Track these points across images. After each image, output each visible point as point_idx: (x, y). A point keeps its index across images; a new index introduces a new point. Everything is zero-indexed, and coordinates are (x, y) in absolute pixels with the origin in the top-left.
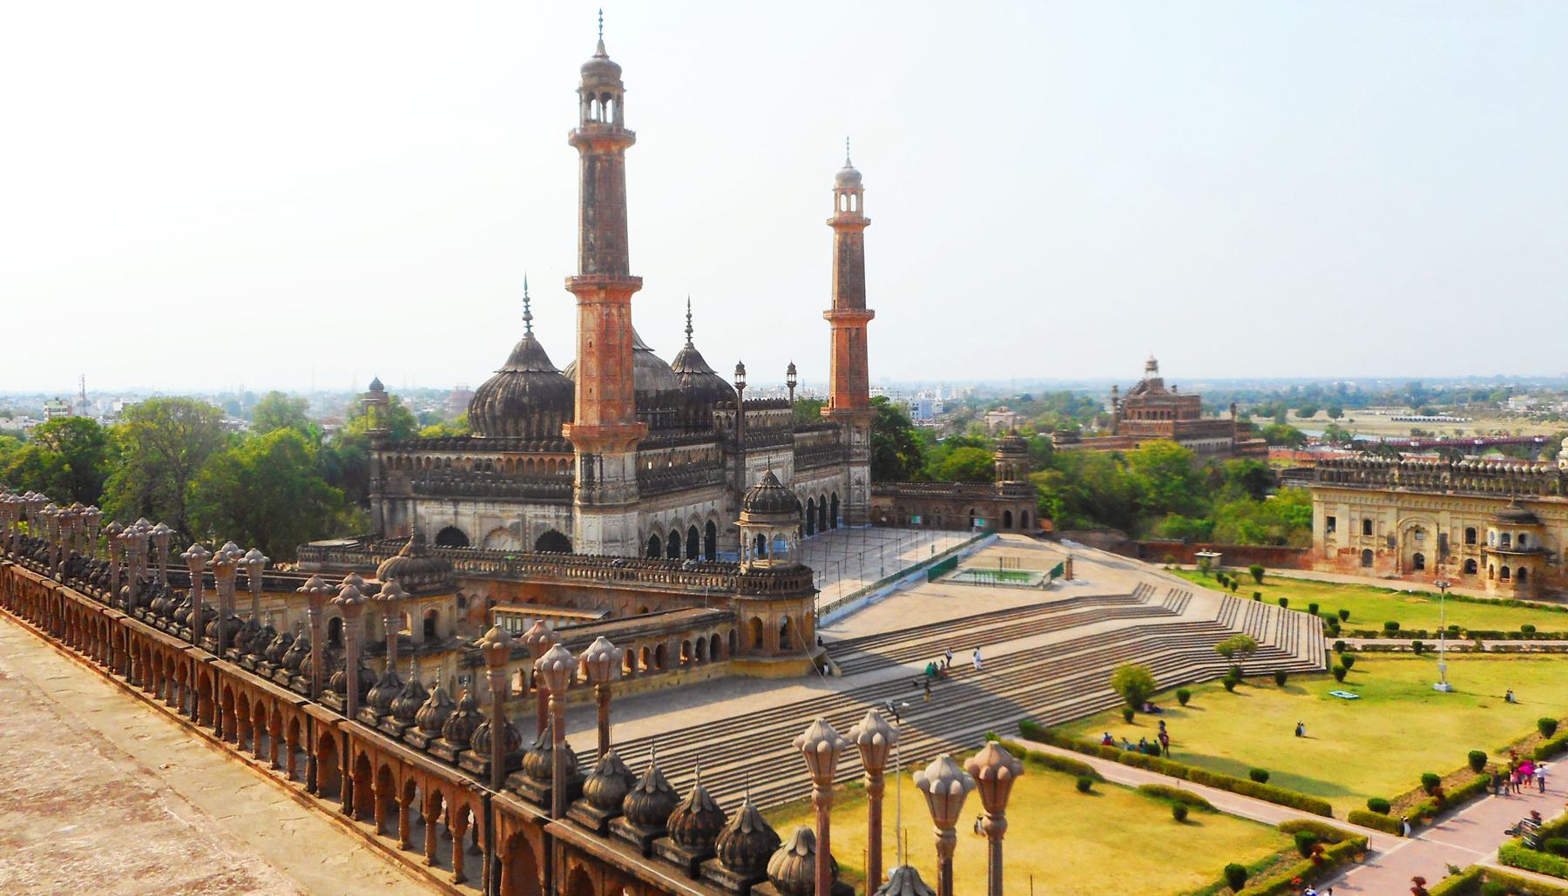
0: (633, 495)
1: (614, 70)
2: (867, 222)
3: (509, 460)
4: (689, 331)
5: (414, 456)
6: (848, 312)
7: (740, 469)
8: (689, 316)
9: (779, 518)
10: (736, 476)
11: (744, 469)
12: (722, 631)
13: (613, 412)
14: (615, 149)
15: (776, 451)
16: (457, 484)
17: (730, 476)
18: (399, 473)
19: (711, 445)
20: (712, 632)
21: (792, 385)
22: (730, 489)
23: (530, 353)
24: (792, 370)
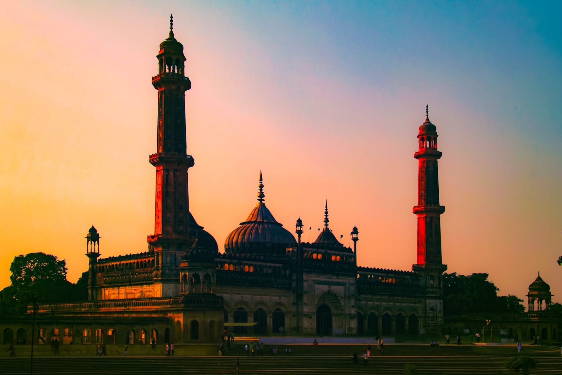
4: (327, 221)
7: (300, 280)
8: (326, 213)
11: (302, 280)
17: (294, 284)
19: (277, 265)
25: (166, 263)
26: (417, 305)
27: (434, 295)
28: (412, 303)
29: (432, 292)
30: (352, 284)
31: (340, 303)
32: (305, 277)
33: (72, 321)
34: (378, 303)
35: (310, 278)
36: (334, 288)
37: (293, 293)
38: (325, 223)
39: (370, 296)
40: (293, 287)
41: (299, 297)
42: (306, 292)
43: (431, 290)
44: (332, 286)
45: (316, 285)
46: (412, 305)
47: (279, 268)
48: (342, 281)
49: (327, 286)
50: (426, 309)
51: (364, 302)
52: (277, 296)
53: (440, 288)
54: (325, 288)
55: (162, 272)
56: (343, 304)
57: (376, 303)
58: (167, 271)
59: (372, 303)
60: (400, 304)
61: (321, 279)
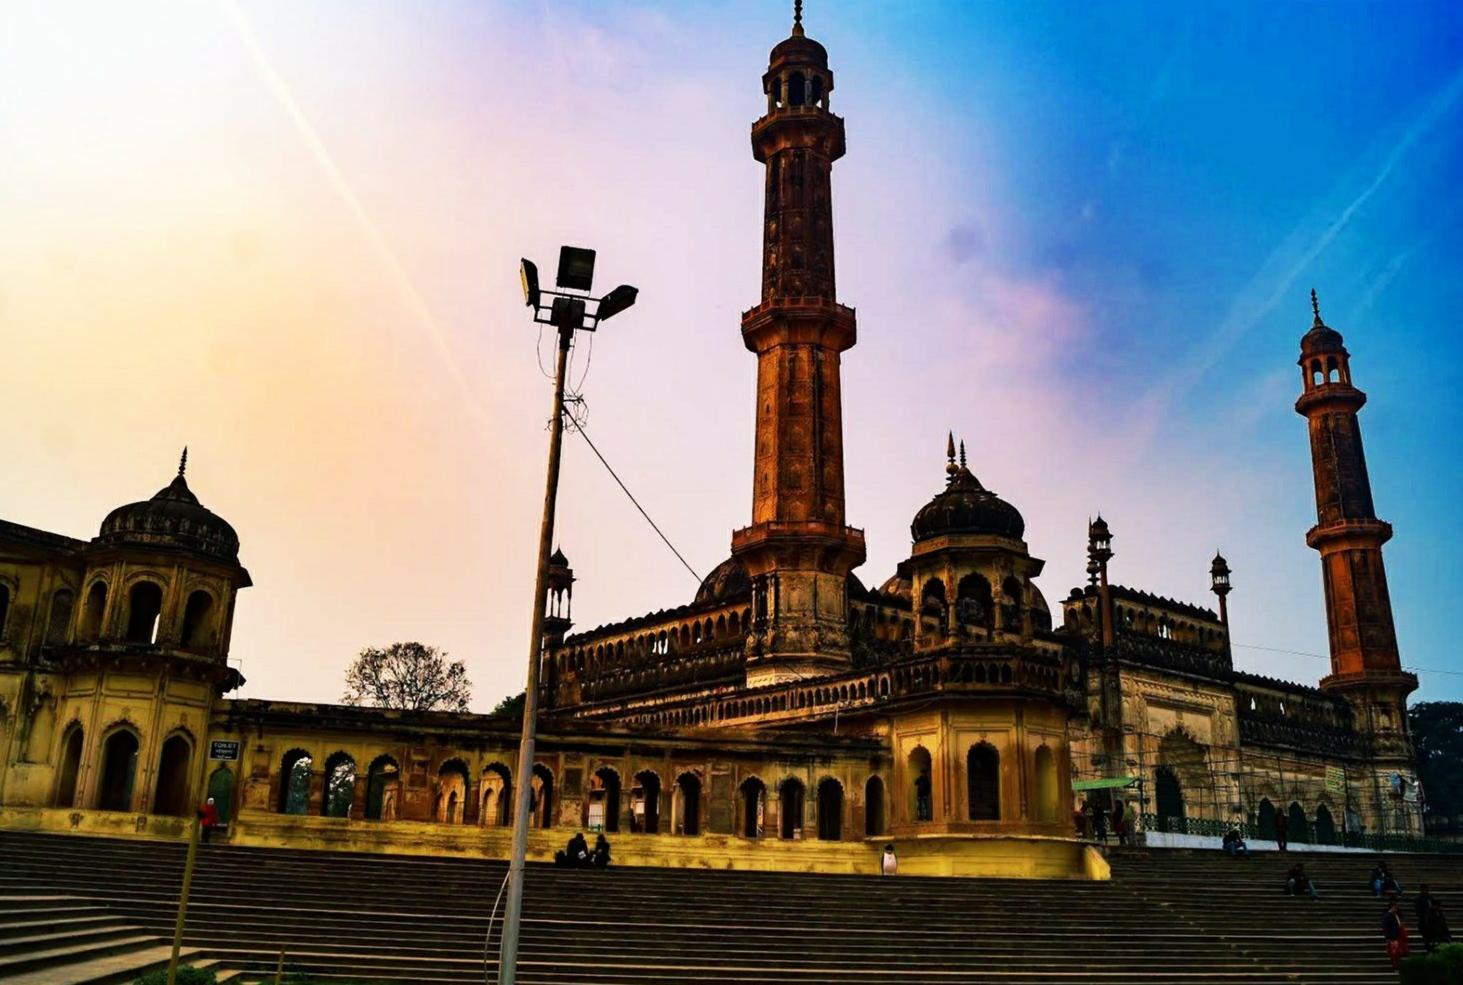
0: (834, 644)
1: (818, 53)
2: (1359, 399)
3: (685, 628)
5: (586, 648)
6: (1342, 526)
7: (1112, 692)
9: (969, 542)
10: (1104, 703)
12: (850, 778)
13: (800, 509)
14: (808, 140)
15: (1195, 683)
16: (627, 677)
17: (1094, 704)
18: (570, 676)
20: (821, 773)
21: (1222, 590)
22: (1095, 726)
24: (1220, 567)
25: (789, 610)
27: (1395, 756)
29: (1391, 749)
30: (1228, 713)
31: (1204, 765)
32: (1126, 682)
33: (554, 739)
36: (1191, 721)
37: (1093, 729)
38: (1090, 576)
39: (1257, 752)
40: (1091, 711)
42: (1131, 728)
43: (1387, 743)
45: (1152, 708)
49: (1171, 714)
50: (1377, 795)
53: (1407, 739)
55: (775, 639)
58: (792, 635)
61: (1161, 692)
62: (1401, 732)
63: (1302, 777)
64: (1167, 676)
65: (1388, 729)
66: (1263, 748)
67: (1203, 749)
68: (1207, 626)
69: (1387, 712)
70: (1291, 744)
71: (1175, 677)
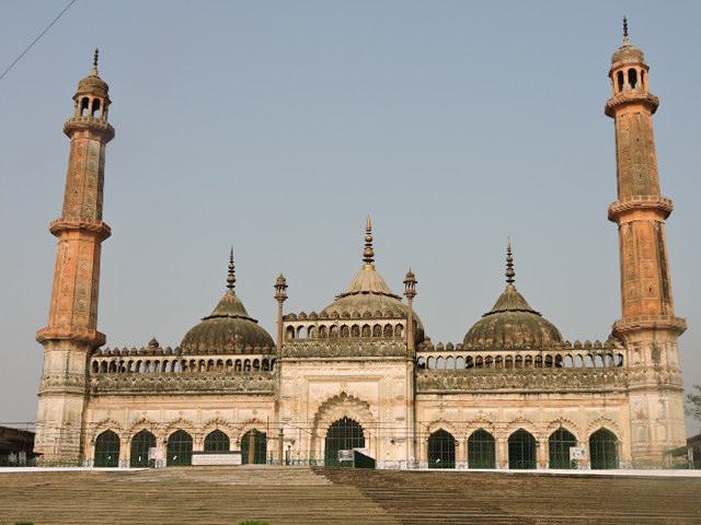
19: (252, 357)
21: (411, 295)
23: (231, 306)
24: (411, 281)
26: (607, 408)
28: (594, 405)
30: (402, 377)
32: (287, 370)
34: (495, 410)
35: (301, 373)
36: (353, 388)
38: (507, 278)
39: (469, 397)
41: (277, 404)
44: (349, 384)
45: (308, 386)
46: (597, 409)
47: (256, 361)
48: (375, 372)
49: (338, 384)
51: (456, 410)
52: (249, 408)
54: (334, 389)
56: (375, 415)
57: (487, 411)
59: (476, 410)
60: (558, 410)
62: (650, 363)
63: (528, 411)
64: (327, 362)
65: (637, 363)
66: (473, 394)
67: (367, 405)
68: (383, 323)
69: (636, 350)
70: (514, 387)
71: (338, 362)
